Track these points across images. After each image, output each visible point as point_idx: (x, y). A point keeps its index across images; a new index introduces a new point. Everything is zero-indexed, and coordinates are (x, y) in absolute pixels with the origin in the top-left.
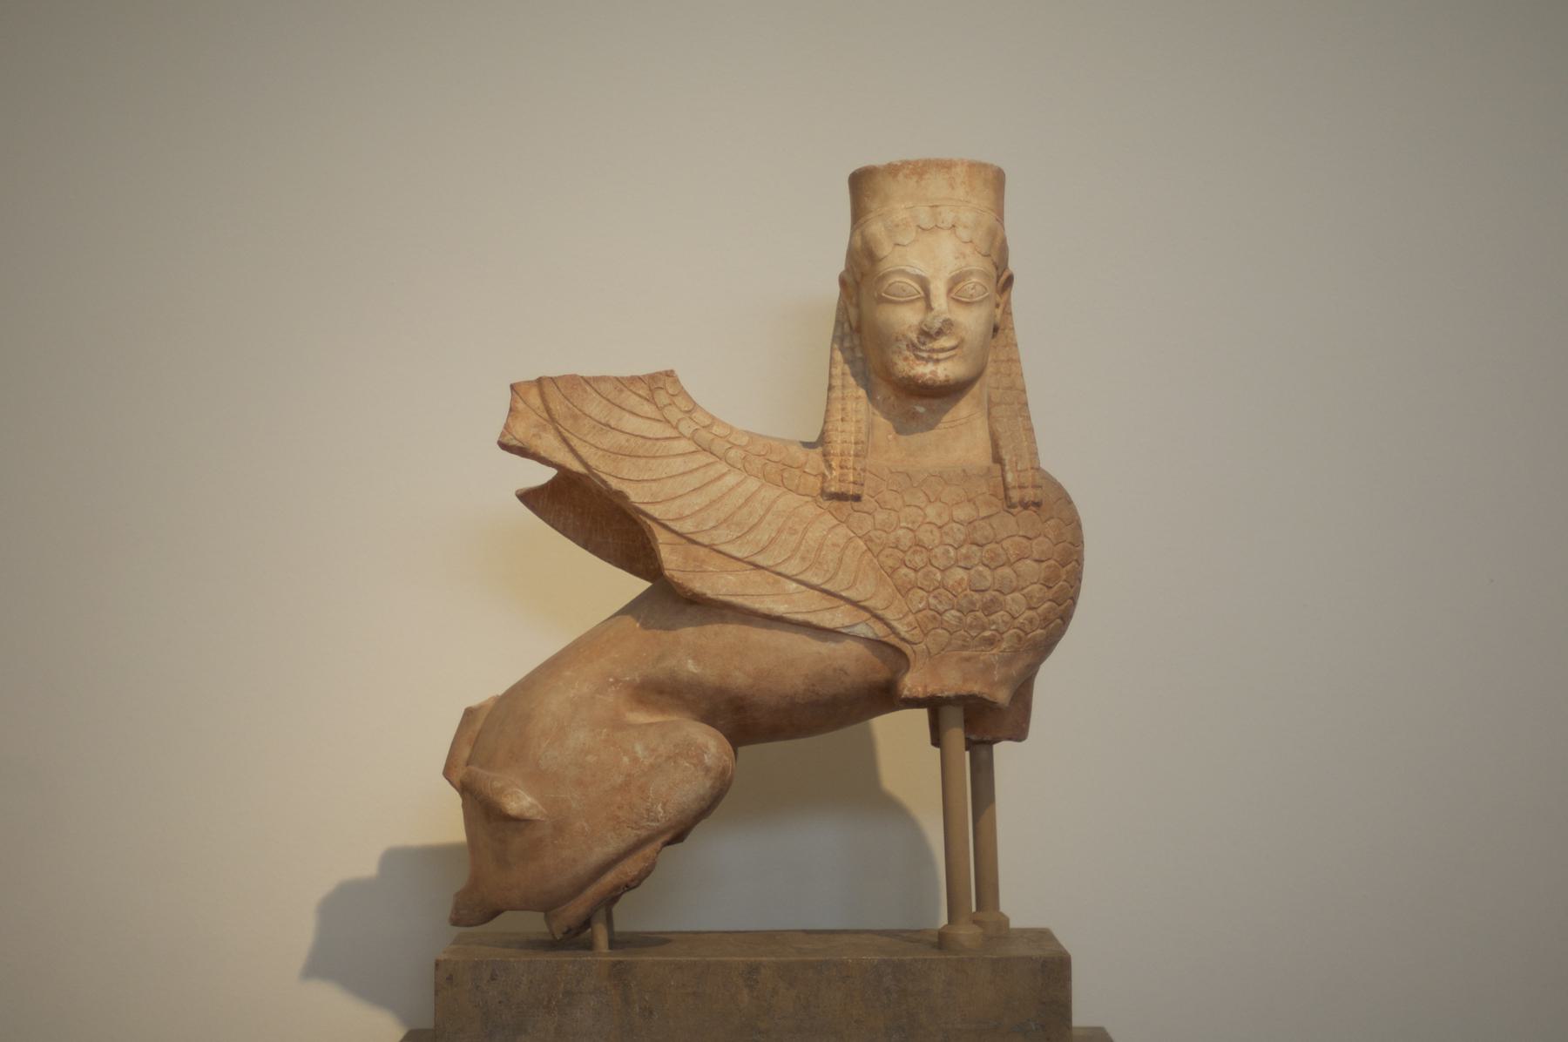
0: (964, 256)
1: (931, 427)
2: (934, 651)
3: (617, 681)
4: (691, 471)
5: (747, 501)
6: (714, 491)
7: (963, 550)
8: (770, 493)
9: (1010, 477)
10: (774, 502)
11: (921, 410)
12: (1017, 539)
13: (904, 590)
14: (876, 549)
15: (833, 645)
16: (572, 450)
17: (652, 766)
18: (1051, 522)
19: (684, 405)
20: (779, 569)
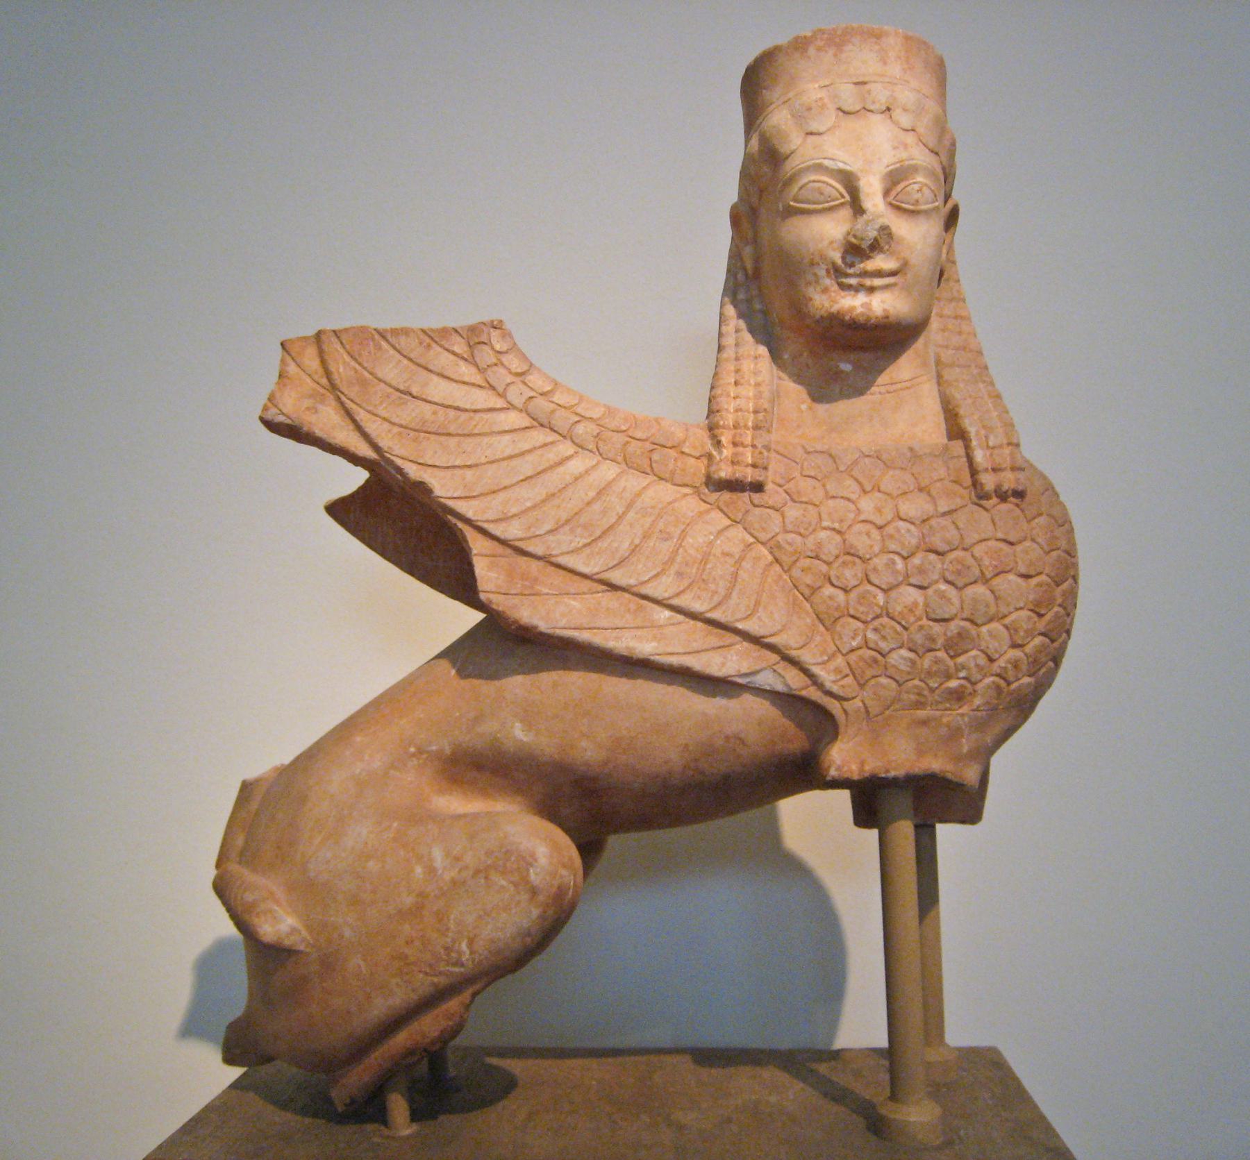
0: (906, 146)
1: (861, 392)
2: (873, 712)
3: (420, 751)
4: (522, 454)
5: (600, 493)
6: (554, 480)
7: (916, 561)
8: (634, 482)
9: (979, 456)
10: (638, 495)
11: (846, 367)
12: (992, 543)
13: (827, 621)
14: (786, 560)
15: (720, 702)
16: (359, 428)
17: (454, 882)
18: (1041, 520)
19: (515, 364)
20: (645, 590)
